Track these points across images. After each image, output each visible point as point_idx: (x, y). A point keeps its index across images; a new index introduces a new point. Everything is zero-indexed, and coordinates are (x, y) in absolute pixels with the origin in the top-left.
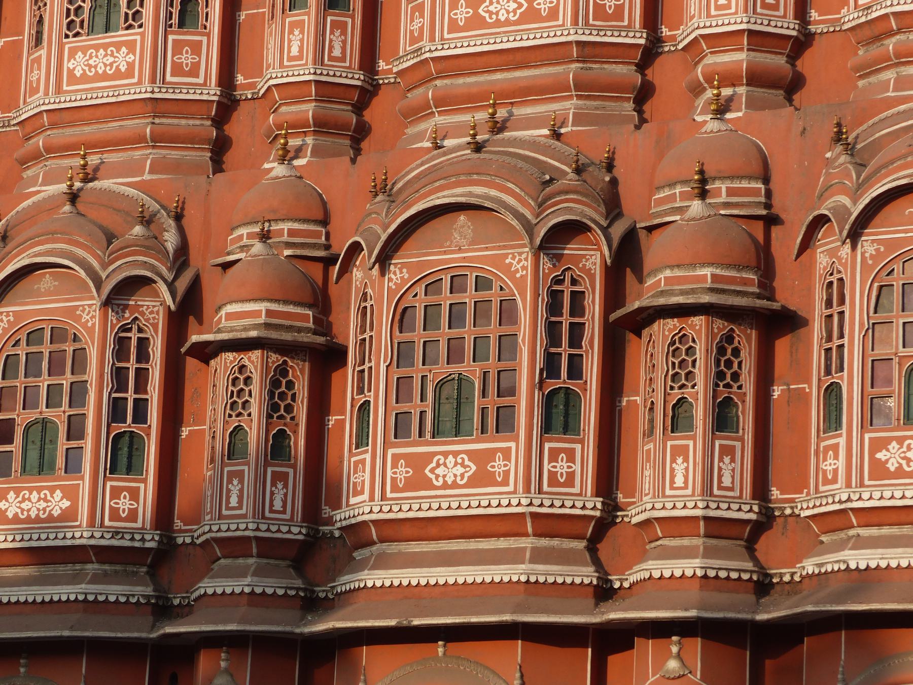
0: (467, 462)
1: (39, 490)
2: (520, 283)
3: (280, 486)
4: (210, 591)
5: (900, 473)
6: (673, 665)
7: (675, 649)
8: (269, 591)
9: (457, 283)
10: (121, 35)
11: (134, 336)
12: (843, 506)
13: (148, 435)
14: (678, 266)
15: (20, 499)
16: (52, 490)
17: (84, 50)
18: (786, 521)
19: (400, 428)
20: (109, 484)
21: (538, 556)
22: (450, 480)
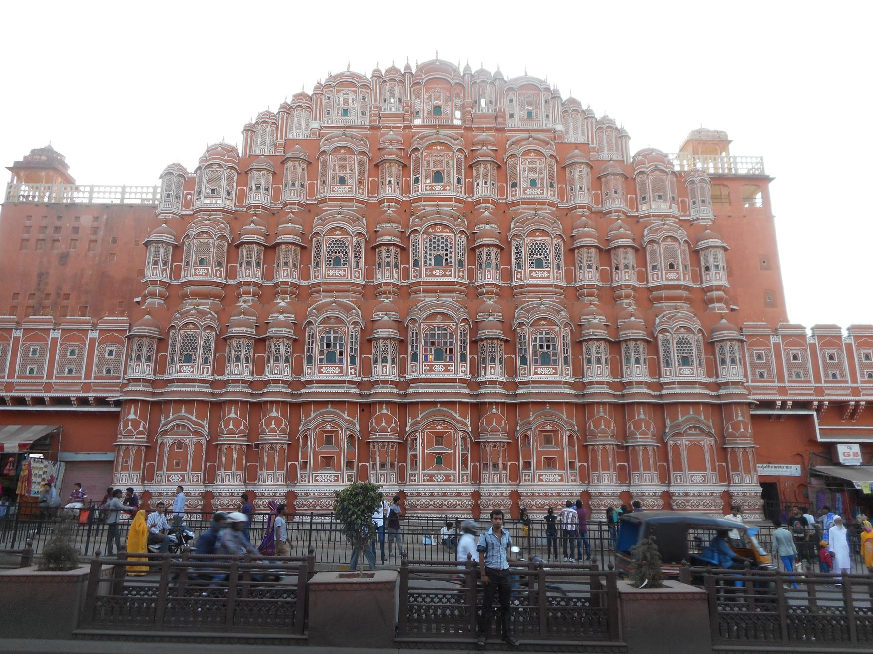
6: (494, 411)
9: (439, 329)
10: (342, 267)
21: (460, 387)
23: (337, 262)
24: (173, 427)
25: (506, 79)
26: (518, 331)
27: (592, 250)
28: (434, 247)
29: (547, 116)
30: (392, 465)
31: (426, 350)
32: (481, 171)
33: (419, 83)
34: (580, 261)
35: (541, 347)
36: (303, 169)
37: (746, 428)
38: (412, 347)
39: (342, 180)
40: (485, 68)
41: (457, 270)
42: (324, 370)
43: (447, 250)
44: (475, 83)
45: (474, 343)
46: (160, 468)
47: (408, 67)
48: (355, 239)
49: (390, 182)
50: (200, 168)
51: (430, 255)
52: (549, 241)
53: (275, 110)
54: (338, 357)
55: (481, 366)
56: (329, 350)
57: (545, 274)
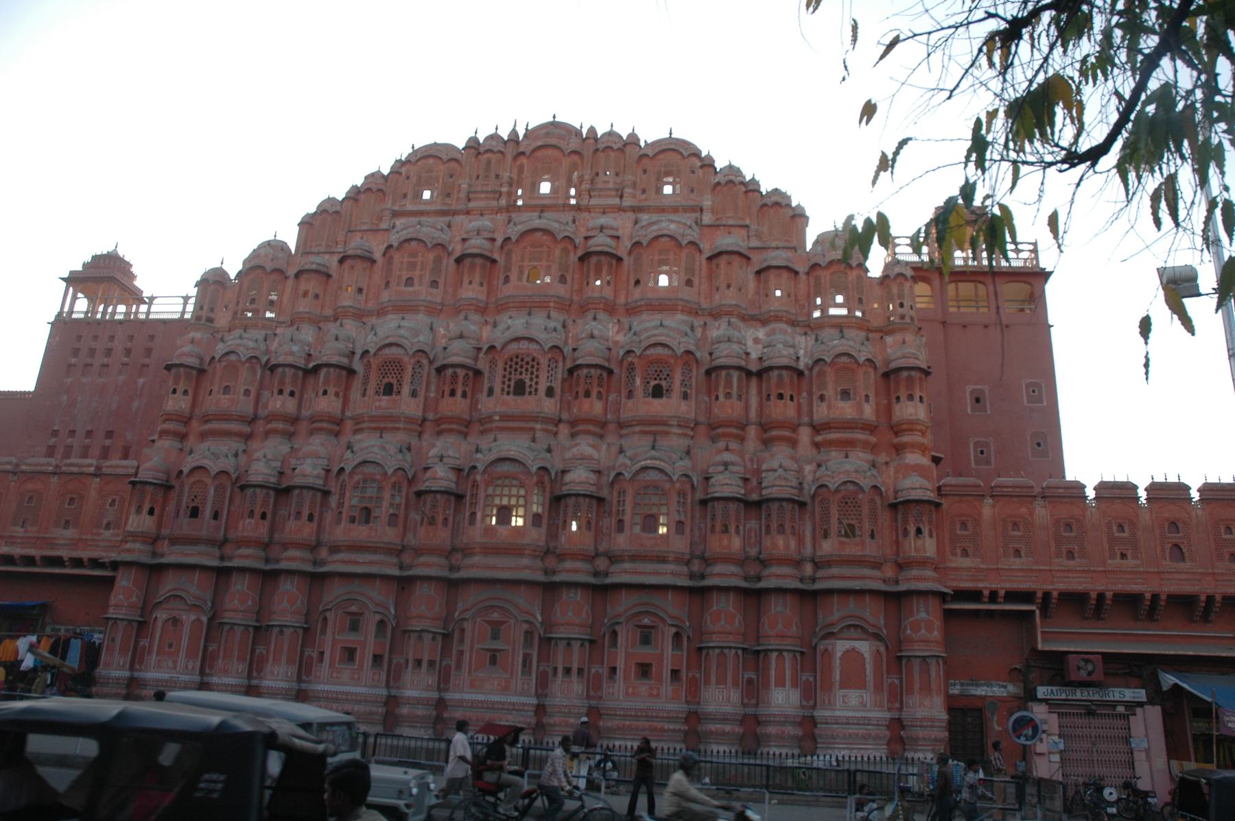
23: (388, 390)
24: (167, 599)
25: (642, 144)
30: (431, 663)
33: (523, 153)
34: (717, 390)
37: (930, 629)
39: (410, 281)
40: (615, 129)
44: (597, 150)
46: (150, 652)
47: (514, 132)
49: (470, 283)
50: (239, 274)
51: (510, 380)
53: (340, 197)
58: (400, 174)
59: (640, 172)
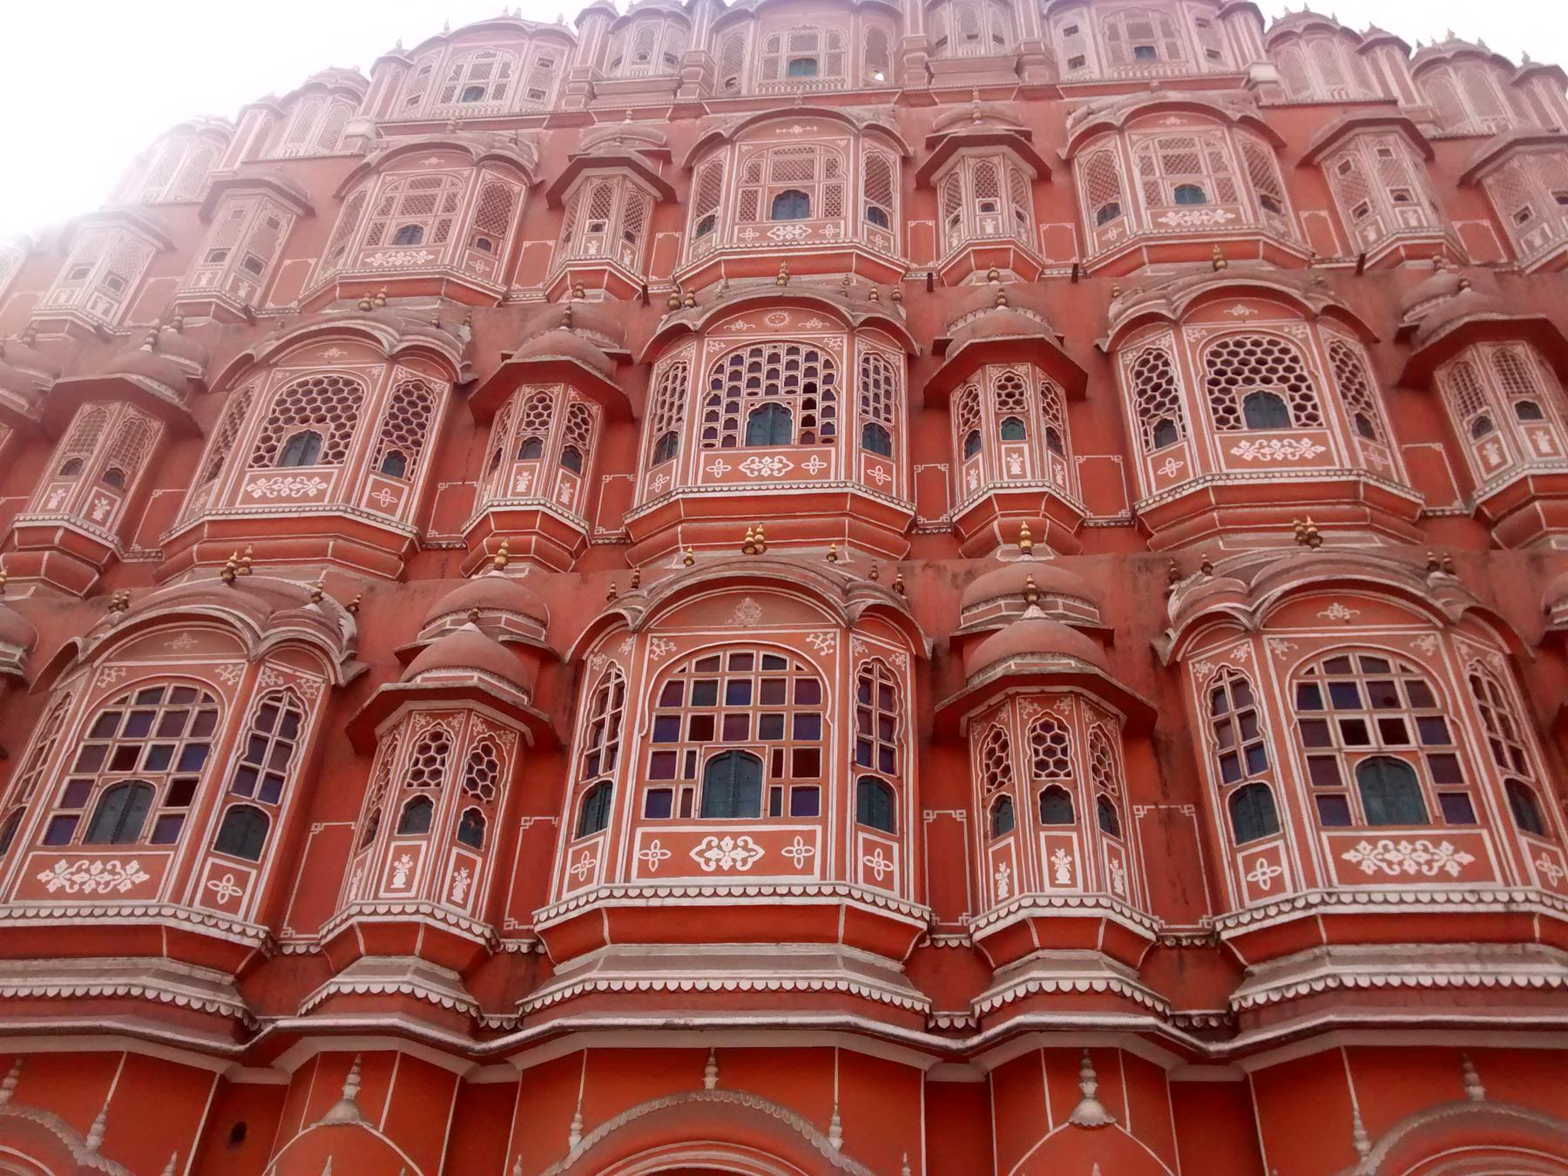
0: (751, 845)
1: (105, 860)
2: (828, 662)
3: (464, 873)
4: (346, 989)
5: (1379, 877)
6: (1090, 1111)
7: (1089, 1088)
8: (434, 998)
10: (318, 468)
11: (283, 707)
12: (1313, 911)
13: (276, 817)
14: (1032, 654)
15: (74, 869)
16: (125, 861)
17: (268, 478)
18: (1181, 956)
19: (658, 804)
20: (211, 860)
22: (726, 866)
23: (302, 449)
26: (1200, 669)
27: (1522, 350)
28: (754, 382)
29: (1213, 55)
31: (663, 764)
32: (967, 180)
34: (1472, 398)
35: (1354, 733)
36: (273, 223)
38: (593, 759)
39: (409, 235)
41: (861, 456)
42: (56, 877)
43: (810, 388)
45: (945, 739)
48: (402, 373)
49: (597, 228)
52: (1296, 332)
54: (158, 807)
55: (985, 852)
56: (124, 776)
57: (1307, 449)
58: (409, 66)
59: (1057, 34)
